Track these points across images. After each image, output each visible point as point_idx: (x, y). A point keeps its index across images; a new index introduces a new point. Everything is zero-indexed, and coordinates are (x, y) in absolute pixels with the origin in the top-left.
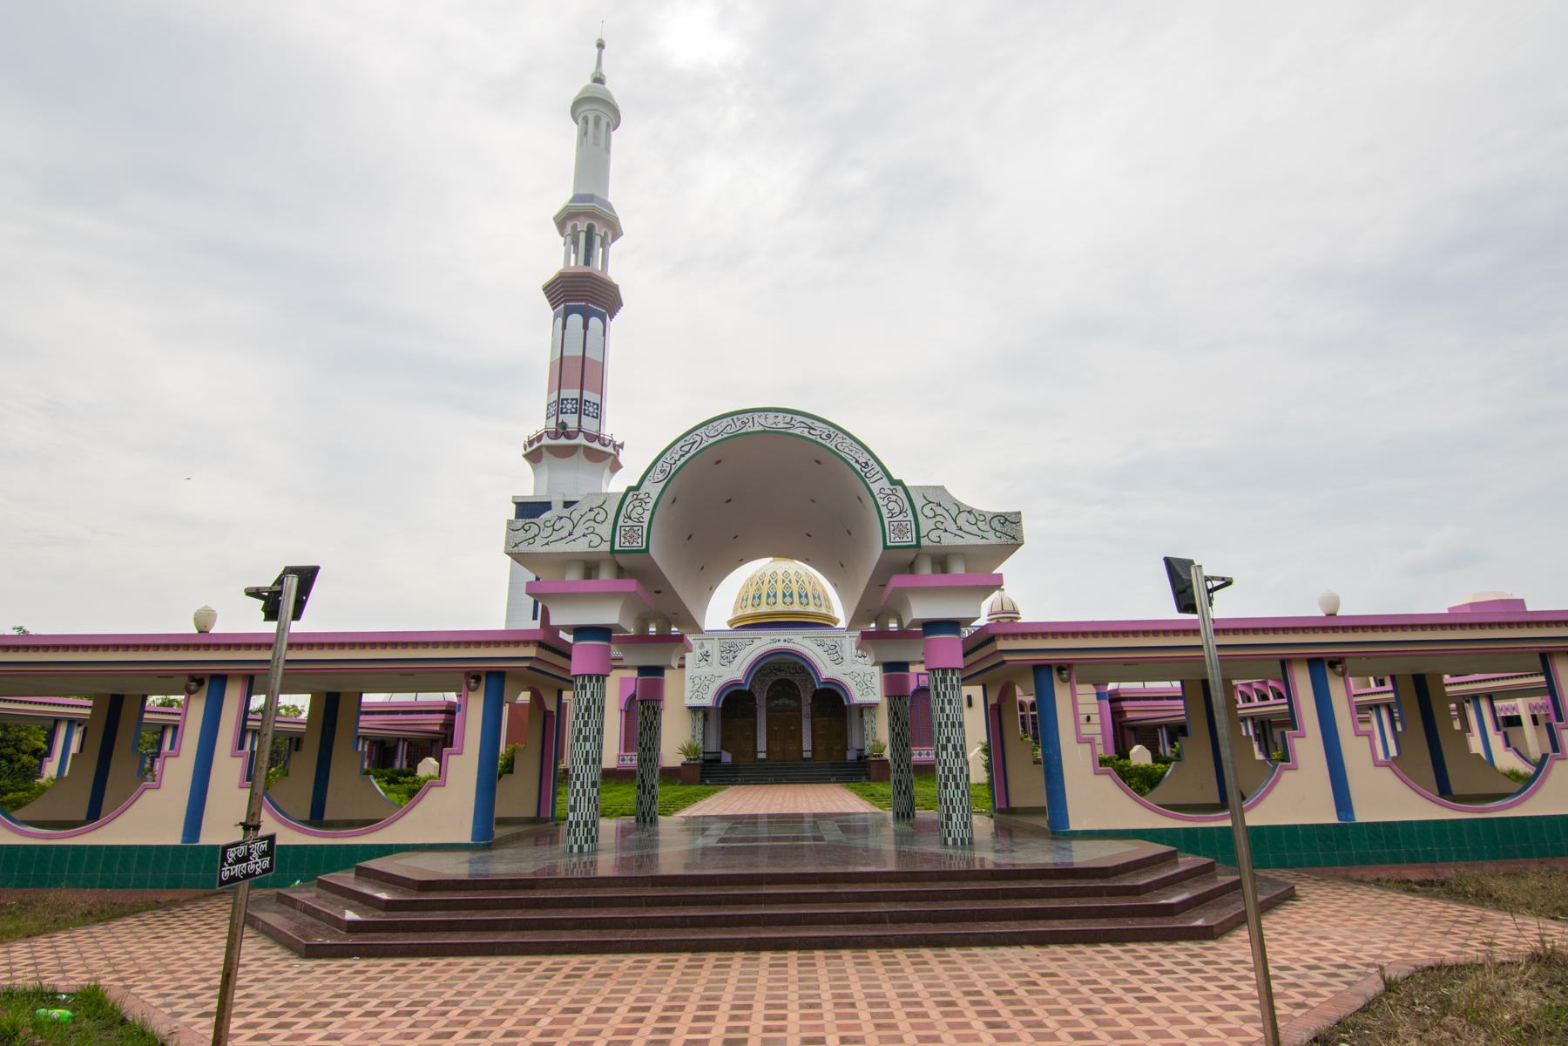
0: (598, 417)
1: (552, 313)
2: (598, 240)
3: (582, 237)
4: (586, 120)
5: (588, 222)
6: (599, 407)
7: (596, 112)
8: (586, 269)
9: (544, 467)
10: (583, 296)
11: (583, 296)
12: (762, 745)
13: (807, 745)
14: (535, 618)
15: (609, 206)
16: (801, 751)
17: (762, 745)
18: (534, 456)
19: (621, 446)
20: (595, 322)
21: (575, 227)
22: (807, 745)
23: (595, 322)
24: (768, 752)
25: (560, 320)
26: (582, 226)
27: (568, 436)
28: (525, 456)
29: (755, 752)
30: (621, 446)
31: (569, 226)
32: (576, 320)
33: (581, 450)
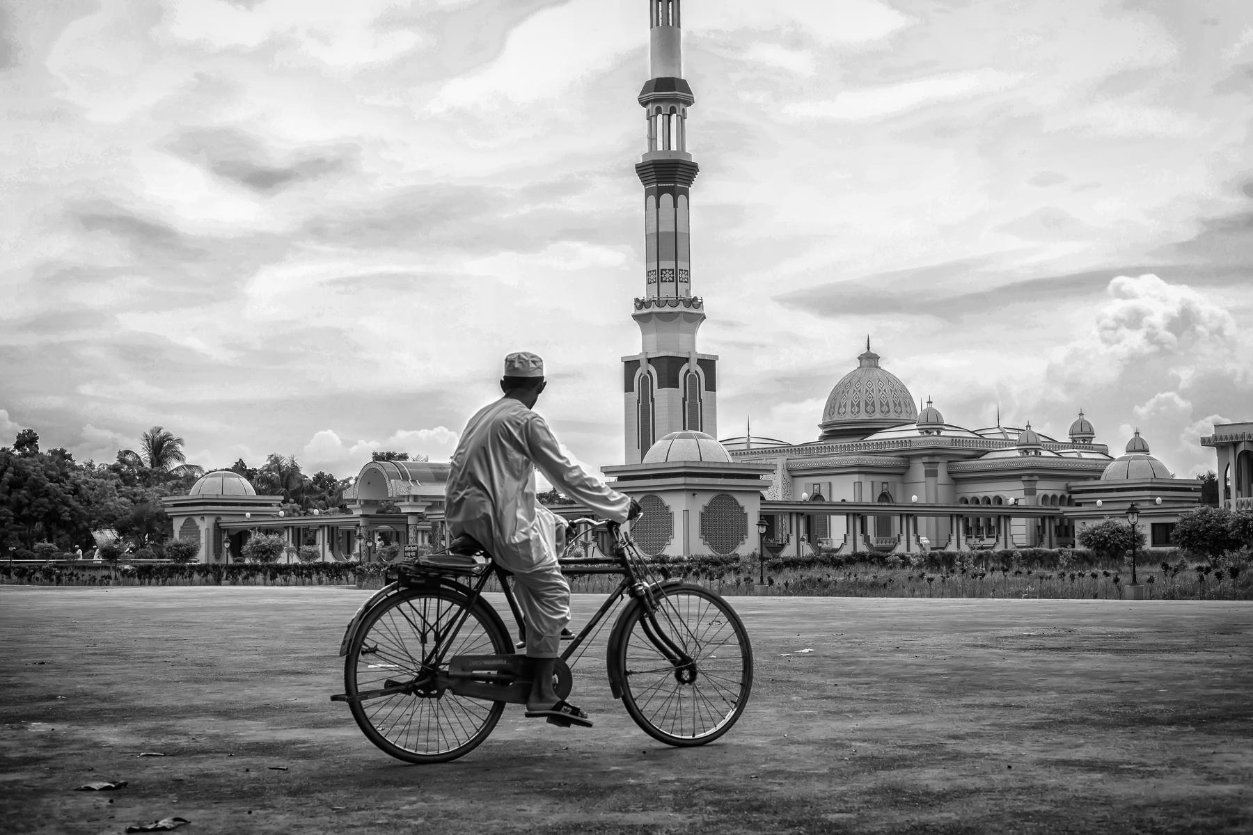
9: (652, 323)
10: (668, 176)
11: (668, 176)
23: (681, 198)
25: (652, 199)
28: (635, 317)
32: (667, 198)
33: (681, 316)
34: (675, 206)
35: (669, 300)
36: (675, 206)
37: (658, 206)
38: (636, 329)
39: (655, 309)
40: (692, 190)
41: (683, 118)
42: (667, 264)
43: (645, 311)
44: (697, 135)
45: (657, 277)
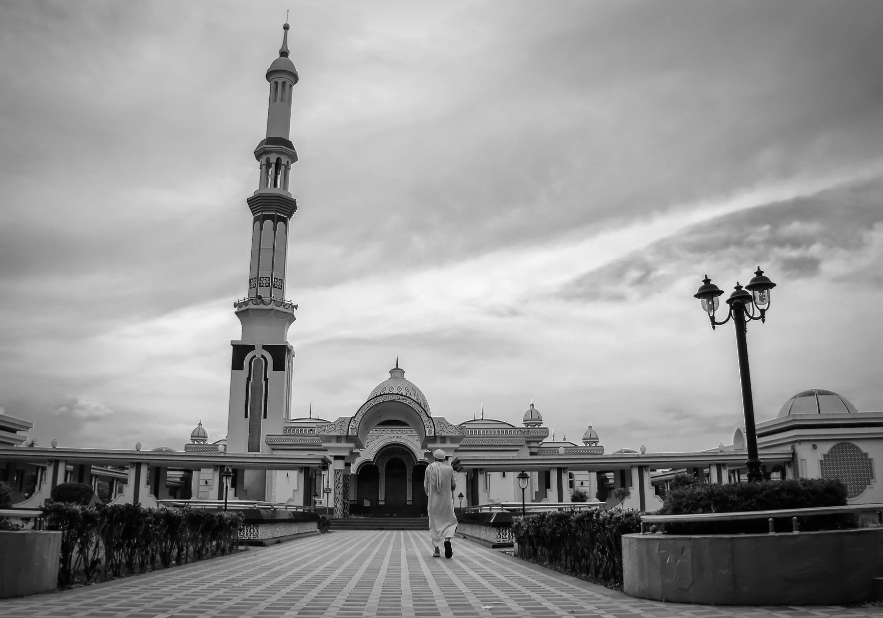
0: (281, 288)
1: (251, 217)
2: (283, 168)
3: (273, 166)
4: (276, 83)
5: (276, 152)
6: (282, 281)
7: (282, 77)
8: (274, 191)
10: (272, 209)
11: (272, 209)
12: (382, 497)
13: (409, 497)
14: (246, 417)
15: (289, 145)
16: (406, 501)
17: (382, 497)
18: (243, 312)
19: (296, 307)
20: (280, 224)
21: (268, 159)
22: (409, 497)
24: (385, 500)
26: (273, 159)
27: (263, 302)
28: (236, 313)
29: (378, 501)
30: (296, 307)
31: (264, 158)
32: (268, 223)
34: (275, 229)
35: (265, 302)
36: (275, 229)
37: (261, 229)
38: (238, 321)
39: (251, 306)
40: (290, 222)
41: (287, 168)
42: (265, 273)
43: (244, 308)
44: (298, 182)
45: (255, 282)
